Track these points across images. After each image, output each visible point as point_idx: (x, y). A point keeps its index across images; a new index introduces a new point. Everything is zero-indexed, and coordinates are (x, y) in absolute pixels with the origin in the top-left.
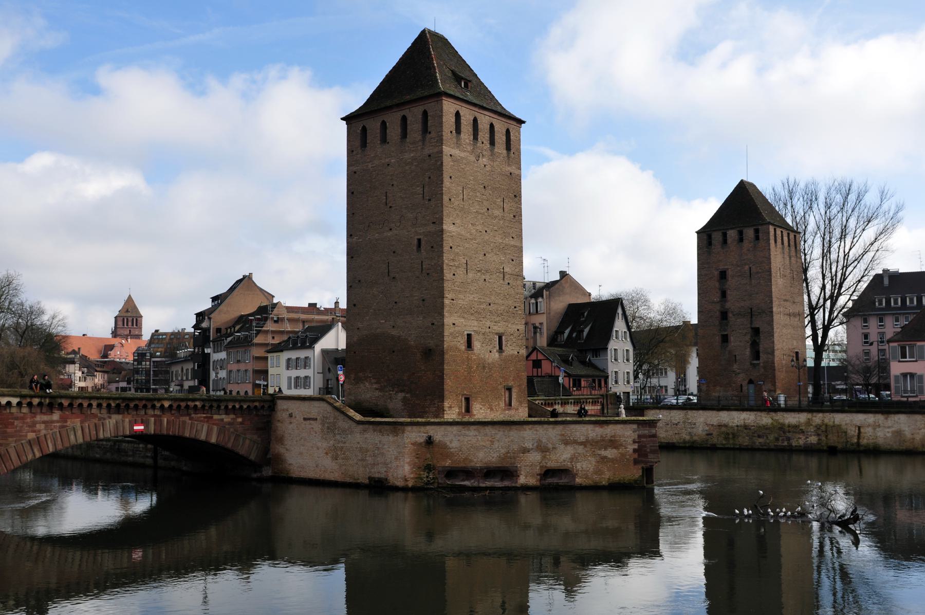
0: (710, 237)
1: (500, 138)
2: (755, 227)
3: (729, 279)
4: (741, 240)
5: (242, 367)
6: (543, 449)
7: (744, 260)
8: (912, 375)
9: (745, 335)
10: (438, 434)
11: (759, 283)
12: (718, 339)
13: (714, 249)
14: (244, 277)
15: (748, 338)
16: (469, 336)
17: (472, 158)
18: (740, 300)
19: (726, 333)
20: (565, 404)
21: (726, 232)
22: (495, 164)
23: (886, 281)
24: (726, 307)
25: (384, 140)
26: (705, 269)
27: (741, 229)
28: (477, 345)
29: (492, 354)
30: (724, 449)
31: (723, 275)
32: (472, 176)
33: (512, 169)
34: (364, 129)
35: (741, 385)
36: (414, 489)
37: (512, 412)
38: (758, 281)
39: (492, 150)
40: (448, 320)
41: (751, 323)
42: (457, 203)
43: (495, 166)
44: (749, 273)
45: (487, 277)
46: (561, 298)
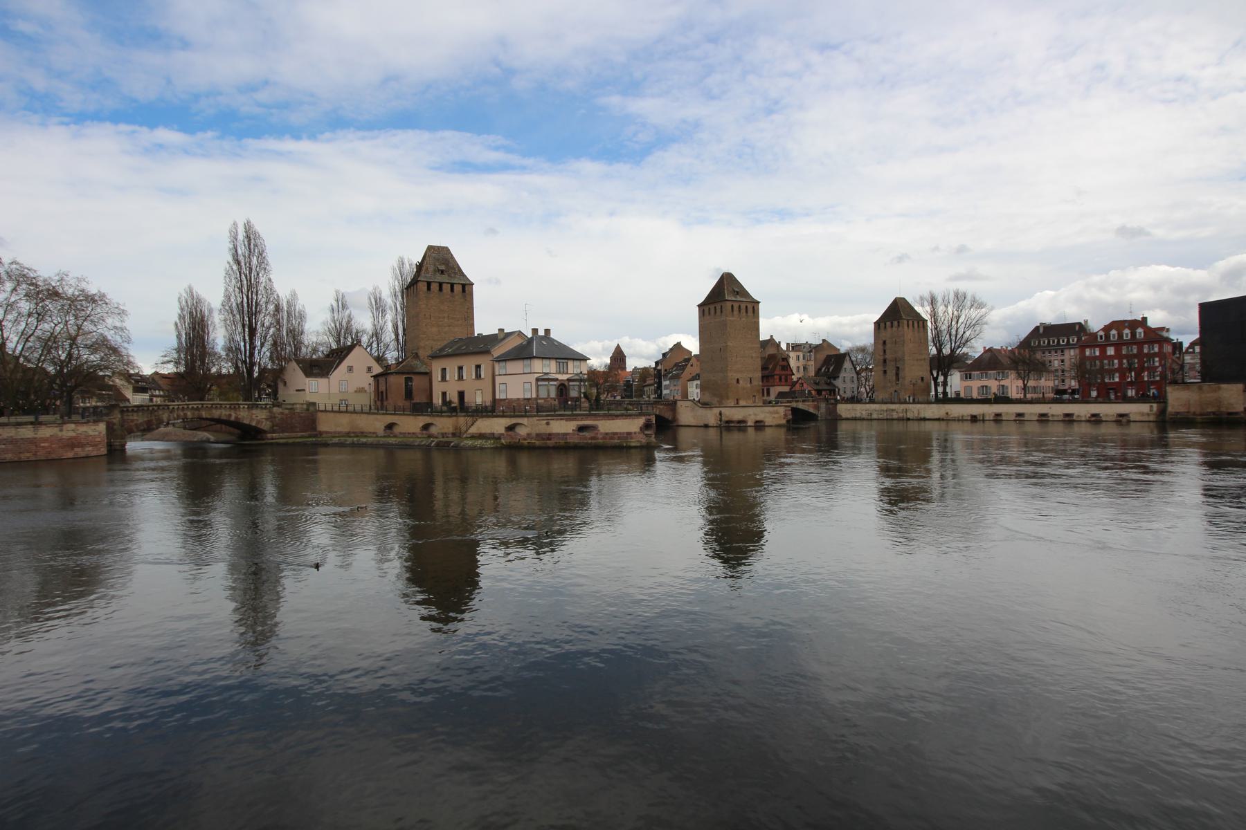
1: (750, 310)
4: (892, 326)
5: (677, 388)
6: (755, 415)
8: (986, 386)
10: (723, 410)
12: (882, 372)
14: (678, 343)
15: (894, 372)
16: (738, 379)
23: (1041, 330)
25: (709, 313)
28: (741, 382)
30: (868, 420)
31: (884, 343)
34: (704, 310)
36: (716, 427)
39: (747, 315)
40: (729, 374)
41: (896, 364)
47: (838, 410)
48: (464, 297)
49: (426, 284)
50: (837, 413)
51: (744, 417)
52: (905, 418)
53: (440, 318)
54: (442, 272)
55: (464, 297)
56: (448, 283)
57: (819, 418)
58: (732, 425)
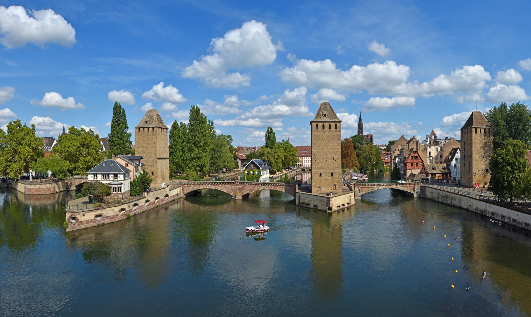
4: (468, 133)
12: (463, 164)
15: (468, 165)
17: (322, 133)
20: (397, 185)
22: (331, 133)
28: (323, 175)
29: (329, 177)
32: (322, 137)
33: (338, 133)
37: (336, 190)
42: (316, 145)
43: (331, 133)
45: (327, 160)
46: (450, 147)
47: (426, 192)
48: (153, 133)
49: (138, 129)
50: (426, 193)
51: (309, 201)
52: (452, 205)
53: (143, 144)
54: (147, 122)
55: (153, 133)
56: (146, 127)
57: (415, 196)
58: (304, 206)
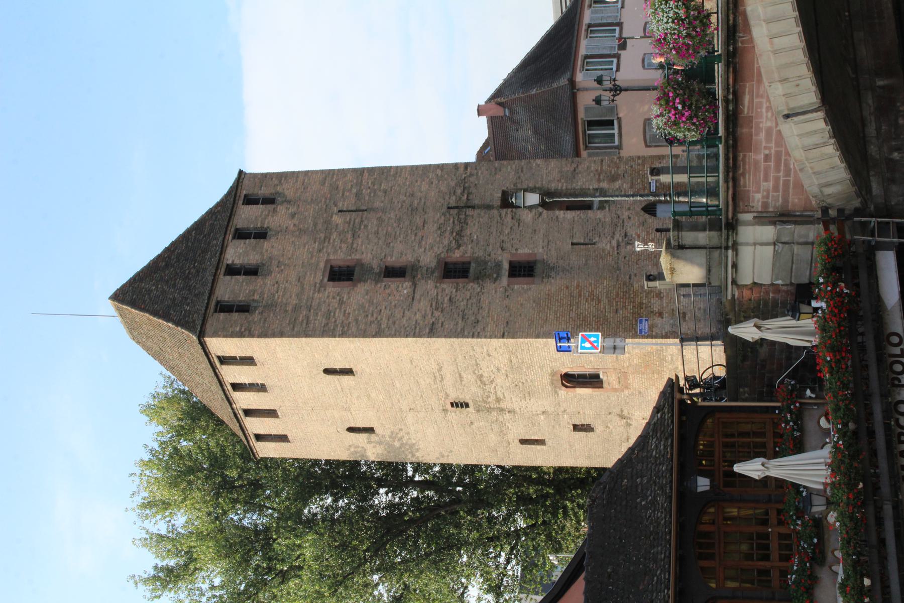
0: (225, 308)
2: (241, 202)
3: (358, 257)
7: (315, 225)
9: (519, 221)
11: (385, 192)
12: (520, 285)
13: (262, 294)
18: (420, 234)
19: (506, 266)
21: (228, 265)
24: (433, 264)
26: (311, 318)
27: (233, 230)
35: (657, 230)
38: (380, 194)
41: (489, 207)
44: (354, 214)
